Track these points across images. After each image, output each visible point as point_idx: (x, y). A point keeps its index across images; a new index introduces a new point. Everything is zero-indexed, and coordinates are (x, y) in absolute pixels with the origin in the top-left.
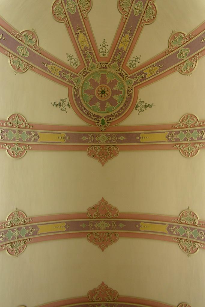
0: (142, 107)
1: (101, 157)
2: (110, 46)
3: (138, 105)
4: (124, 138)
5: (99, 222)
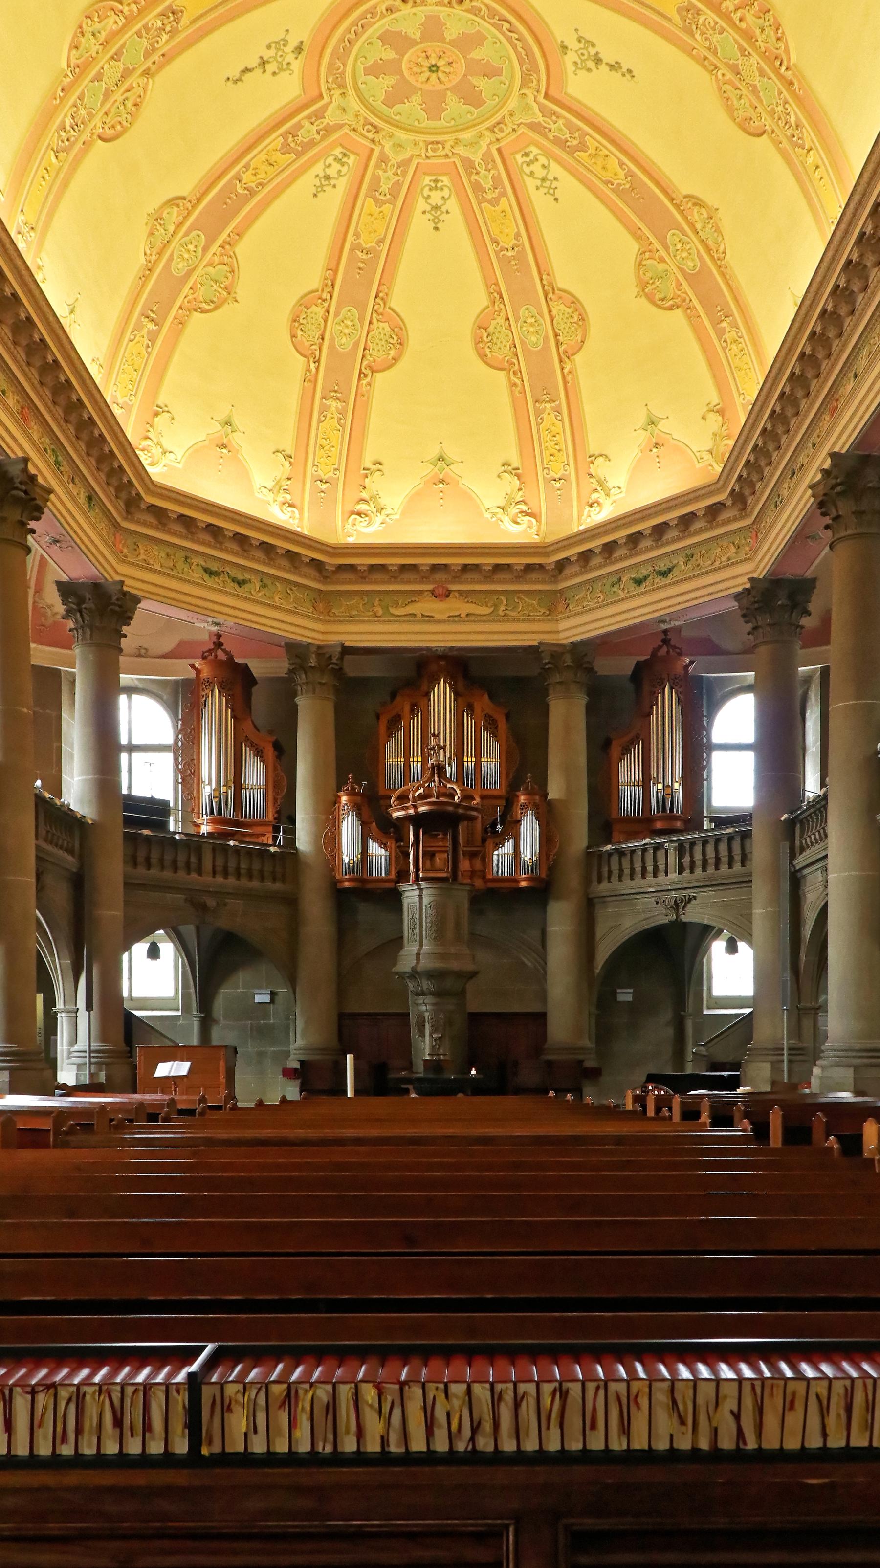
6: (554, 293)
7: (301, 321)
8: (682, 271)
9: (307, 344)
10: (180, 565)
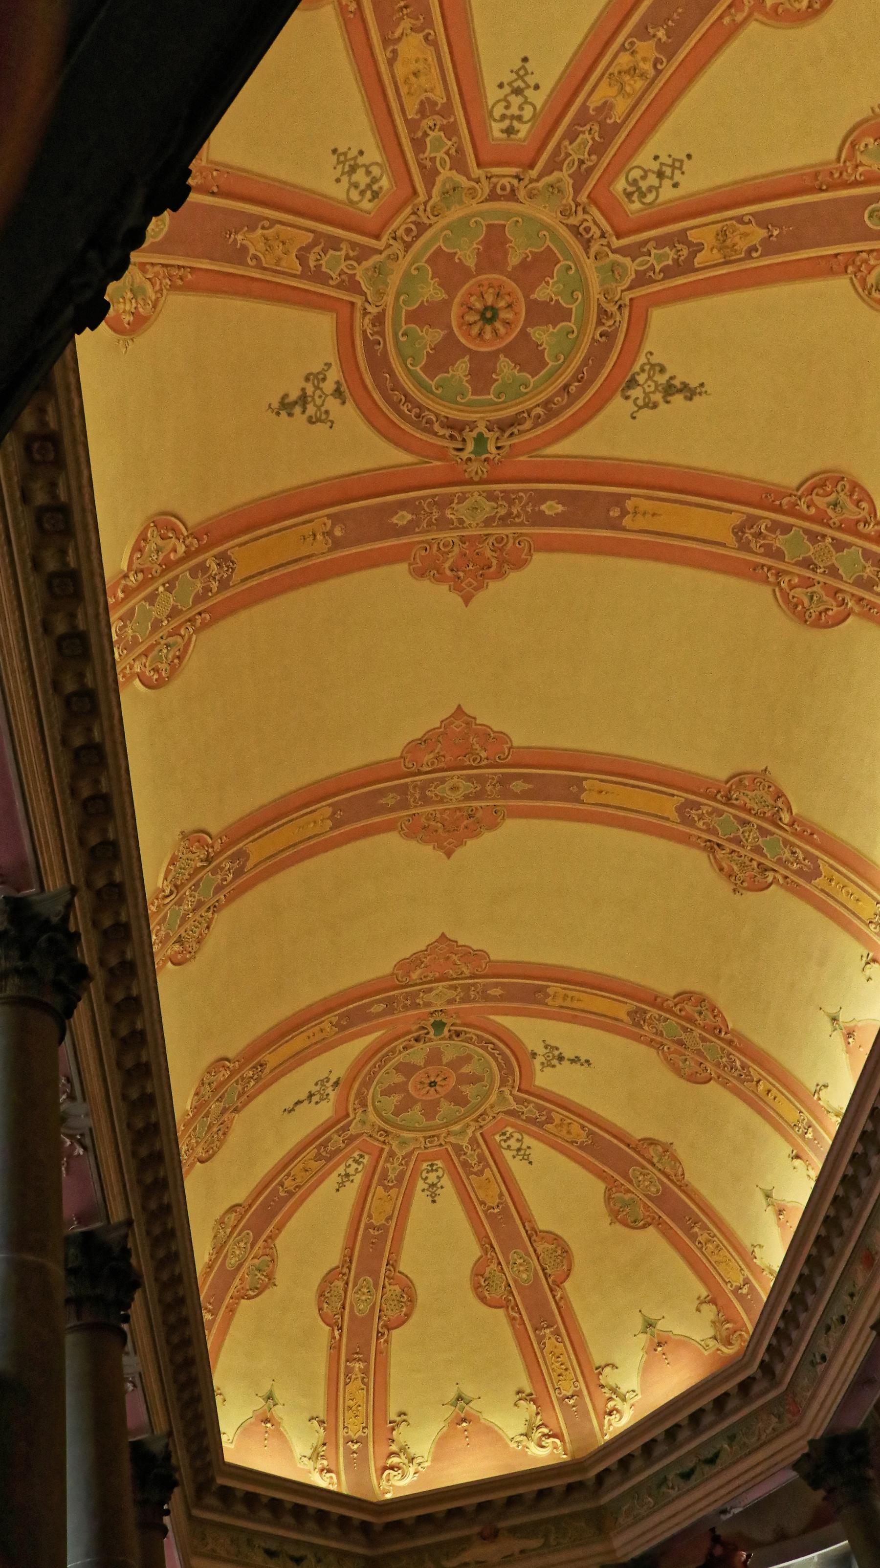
0: (652, 389)
2: (547, 87)
3: (637, 378)
6: (537, 1235)
7: (327, 1295)
8: (646, 1196)
9: (331, 1314)
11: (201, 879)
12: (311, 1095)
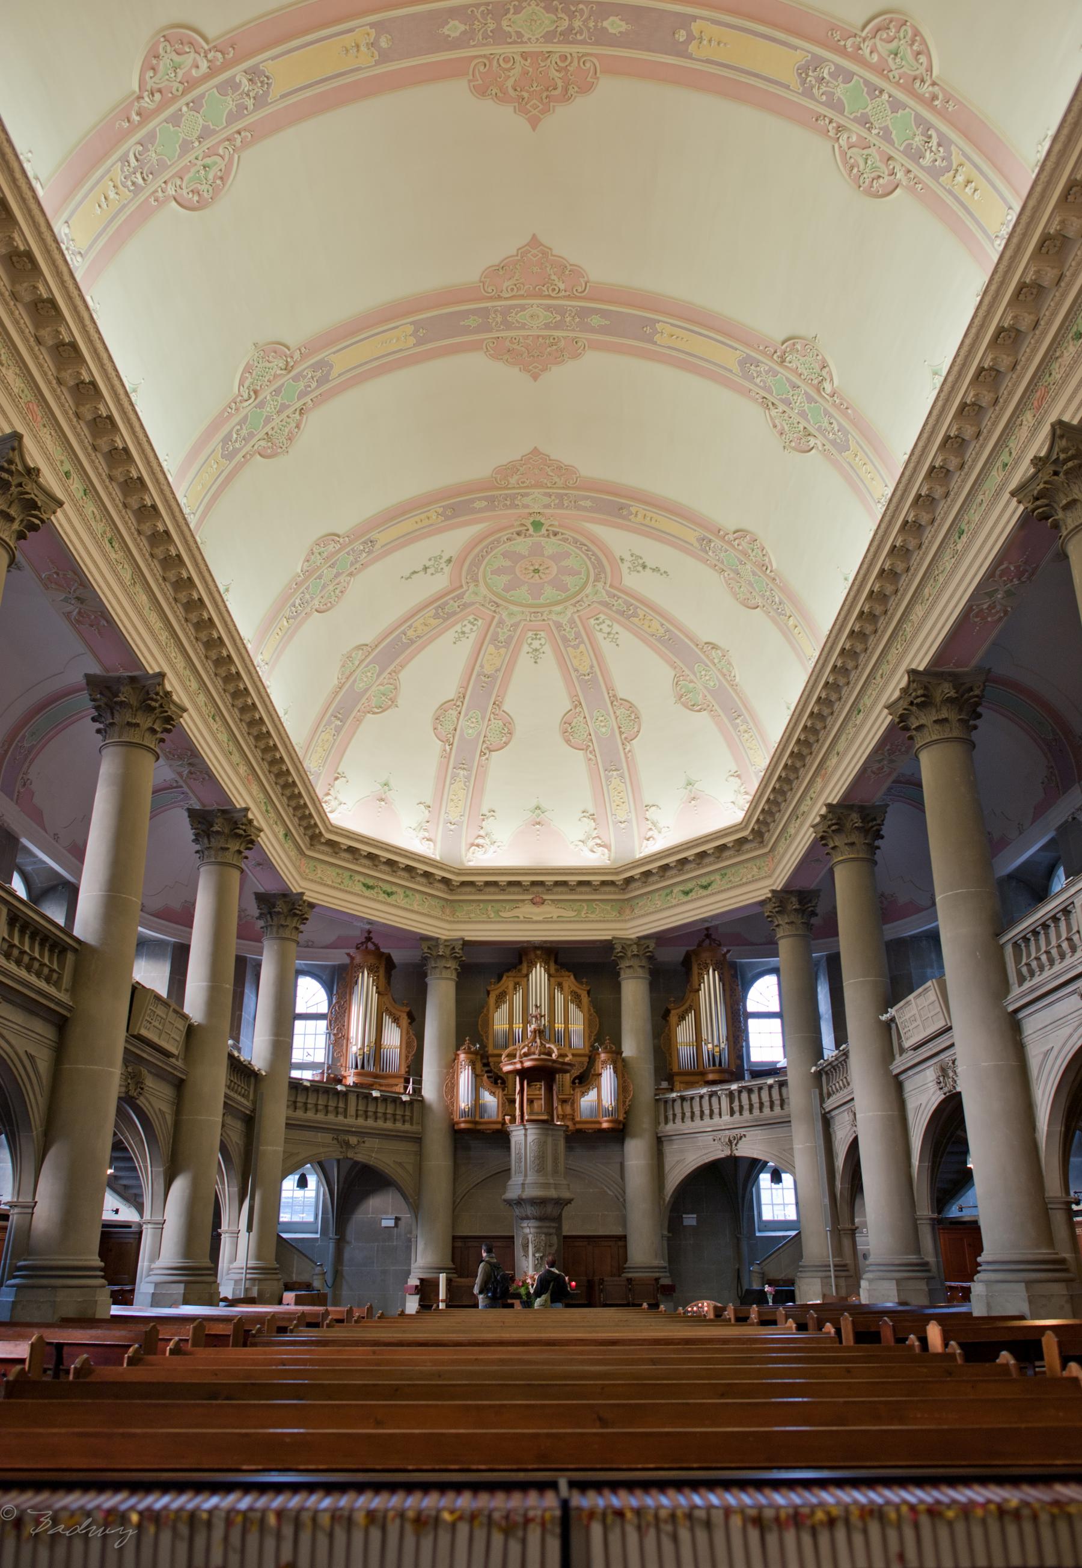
1: (526, 95)
4: (623, 23)
5: (523, 308)
8: (706, 688)
9: (444, 734)
10: (347, 881)
11: (283, 385)
12: (426, 568)
